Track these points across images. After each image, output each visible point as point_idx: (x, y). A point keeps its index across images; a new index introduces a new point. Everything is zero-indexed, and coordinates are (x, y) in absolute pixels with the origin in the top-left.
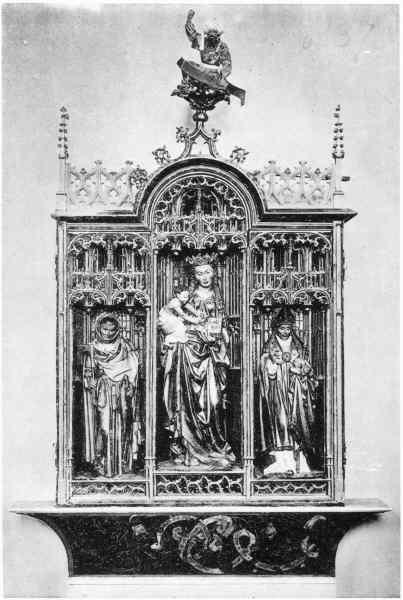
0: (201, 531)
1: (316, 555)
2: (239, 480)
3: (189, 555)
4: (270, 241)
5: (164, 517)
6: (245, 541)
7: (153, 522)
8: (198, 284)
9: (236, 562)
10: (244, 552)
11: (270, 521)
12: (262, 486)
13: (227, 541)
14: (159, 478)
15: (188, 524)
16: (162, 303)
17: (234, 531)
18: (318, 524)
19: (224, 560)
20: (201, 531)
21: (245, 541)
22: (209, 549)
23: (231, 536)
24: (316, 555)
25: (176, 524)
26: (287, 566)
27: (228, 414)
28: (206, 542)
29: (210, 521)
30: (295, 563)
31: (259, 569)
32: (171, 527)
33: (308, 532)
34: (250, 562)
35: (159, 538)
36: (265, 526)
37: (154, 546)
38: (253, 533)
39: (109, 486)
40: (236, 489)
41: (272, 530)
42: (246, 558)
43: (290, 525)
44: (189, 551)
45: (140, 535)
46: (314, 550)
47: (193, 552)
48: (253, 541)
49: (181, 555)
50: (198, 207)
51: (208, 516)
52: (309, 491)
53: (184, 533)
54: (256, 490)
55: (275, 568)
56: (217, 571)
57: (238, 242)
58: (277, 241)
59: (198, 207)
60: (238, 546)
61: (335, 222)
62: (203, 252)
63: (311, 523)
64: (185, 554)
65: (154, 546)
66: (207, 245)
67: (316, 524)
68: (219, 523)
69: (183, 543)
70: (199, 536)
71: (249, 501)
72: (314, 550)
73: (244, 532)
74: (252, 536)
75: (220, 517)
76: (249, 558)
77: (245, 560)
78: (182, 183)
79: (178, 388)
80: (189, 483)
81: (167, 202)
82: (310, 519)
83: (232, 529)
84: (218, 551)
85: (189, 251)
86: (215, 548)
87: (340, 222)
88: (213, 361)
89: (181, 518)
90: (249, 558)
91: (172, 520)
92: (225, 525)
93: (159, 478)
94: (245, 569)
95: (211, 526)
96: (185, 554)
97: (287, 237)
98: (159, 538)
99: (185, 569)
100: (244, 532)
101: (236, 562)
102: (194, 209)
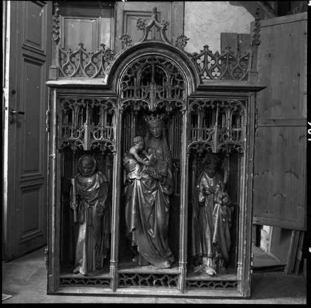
4: (203, 106)
8: (151, 135)
14: (121, 275)
16: (124, 150)
27: (170, 233)
50: (153, 79)
54: (187, 285)
57: (180, 106)
58: (208, 106)
59: (153, 79)
61: (250, 93)
62: (155, 113)
66: (158, 108)
78: (141, 62)
79: (133, 212)
81: (129, 76)
85: (144, 112)
87: (254, 93)
88: (160, 191)
97: (215, 103)
102: (150, 81)
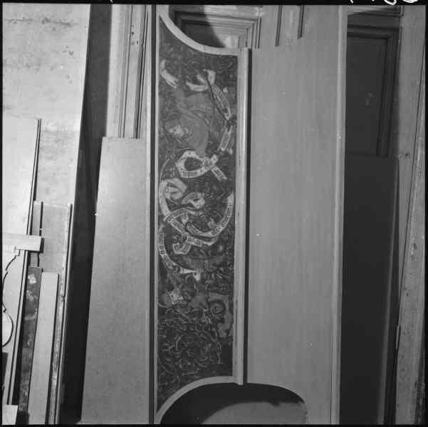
1: (212, 74)
3: (210, 234)
6: (191, 165)
9: (221, 176)
10: (207, 165)
13: (194, 186)
17: (178, 176)
18: (170, 69)
20: (179, 219)
21: (191, 165)
24: (212, 74)
25: (169, 251)
26: (226, 111)
31: (228, 147)
32: (173, 257)
33: (182, 83)
34: (219, 158)
35: (187, 271)
37: (197, 278)
38: (182, 153)
42: (214, 162)
47: (205, 228)
48: (193, 155)
49: (210, 244)
55: (229, 126)
56: (230, 200)
60: (199, 172)
63: (170, 79)
64: (209, 239)
65: (197, 278)
67: (172, 73)
68: (168, 197)
70: (184, 221)
72: (206, 75)
74: (186, 154)
76: (215, 159)
77: (218, 164)
84: (205, 199)
86: (201, 202)
90: (215, 159)
94: (228, 164)
95: (172, 205)
96: (209, 239)
98: (187, 271)
100: (181, 165)
101: (221, 176)
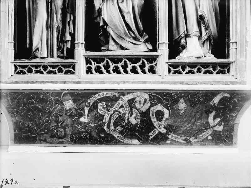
0: (122, 106)
2: (155, 63)
5: (89, 94)
6: (159, 115)
7: (81, 97)
11: (181, 97)
12: (175, 68)
13: (145, 115)
15: (111, 100)
19: (142, 132)
20: (122, 106)
22: (129, 122)
23: (148, 110)
24: (220, 128)
25: (101, 100)
28: (127, 115)
29: (130, 97)
30: (203, 135)
31: (172, 140)
33: (214, 108)
35: (86, 110)
36: (176, 101)
37: (82, 120)
38: (167, 108)
39: (45, 67)
40: (152, 70)
41: (182, 105)
43: (200, 101)
44: (112, 124)
45: (70, 109)
46: (219, 124)
47: (116, 125)
48: (166, 115)
49: (105, 128)
51: (128, 93)
52: (215, 72)
53: (107, 108)
54: (170, 71)
55: (186, 140)
56: (136, 141)
60: (154, 120)
63: (216, 100)
64: (109, 127)
65: (82, 120)
67: (221, 101)
69: (107, 117)
71: (164, 80)
72: (219, 124)
73: (159, 107)
75: (139, 93)
77: (160, 133)
80: (112, 66)
82: (216, 96)
83: (149, 104)
84: (137, 124)
86: (133, 121)
89: (105, 94)
91: (97, 97)
92: (142, 101)
93: (88, 62)
94: (160, 139)
96: (109, 127)
98: (86, 110)
99: (108, 140)
100: (159, 107)
101: (152, 135)
